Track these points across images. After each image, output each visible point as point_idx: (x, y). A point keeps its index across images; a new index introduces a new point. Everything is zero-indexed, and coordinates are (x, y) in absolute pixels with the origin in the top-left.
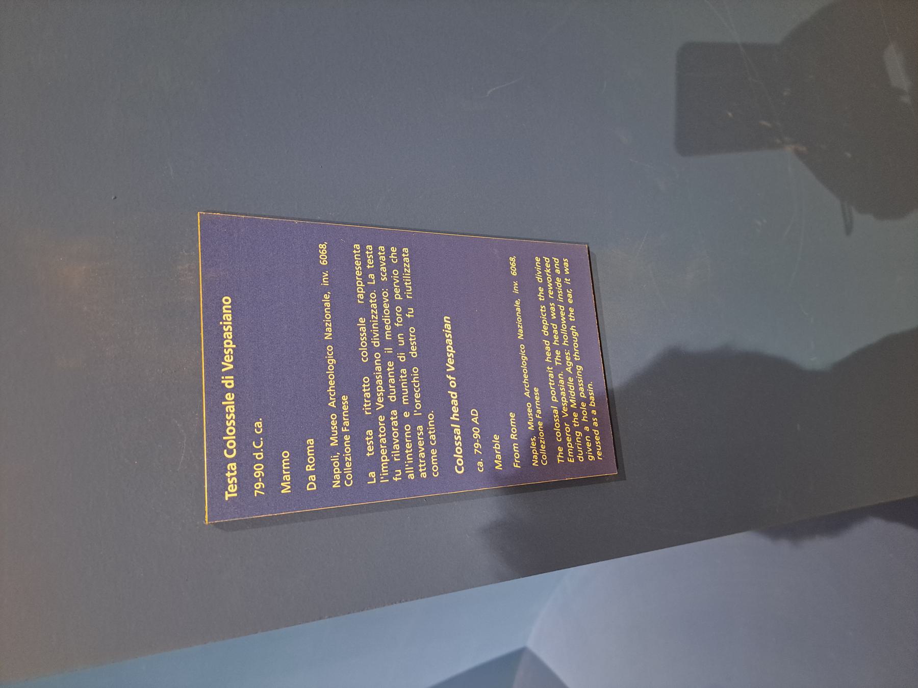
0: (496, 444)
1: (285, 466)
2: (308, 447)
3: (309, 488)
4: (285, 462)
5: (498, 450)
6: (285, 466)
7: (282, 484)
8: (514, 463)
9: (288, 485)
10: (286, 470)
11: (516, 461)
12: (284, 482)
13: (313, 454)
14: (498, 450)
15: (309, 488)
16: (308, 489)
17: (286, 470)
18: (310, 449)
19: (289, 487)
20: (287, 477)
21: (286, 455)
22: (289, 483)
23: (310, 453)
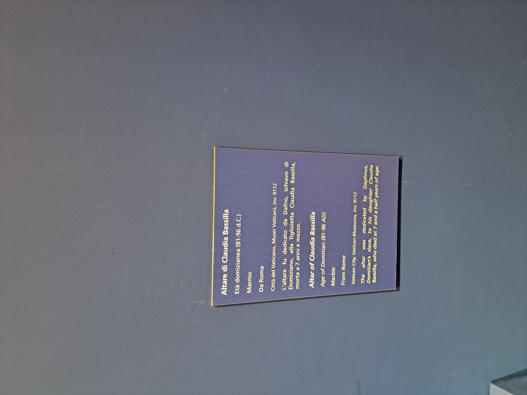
1: (250, 279)
3: (260, 290)
5: (334, 276)
6: (250, 279)
7: (248, 288)
8: (342, 283)
9: (250, 289)
10: (250, 282)
12: (248, 287)
14: (334, 276)
17: (250, 282)
20: (250, 285)
21: (250, 274)
22: (251, 288)
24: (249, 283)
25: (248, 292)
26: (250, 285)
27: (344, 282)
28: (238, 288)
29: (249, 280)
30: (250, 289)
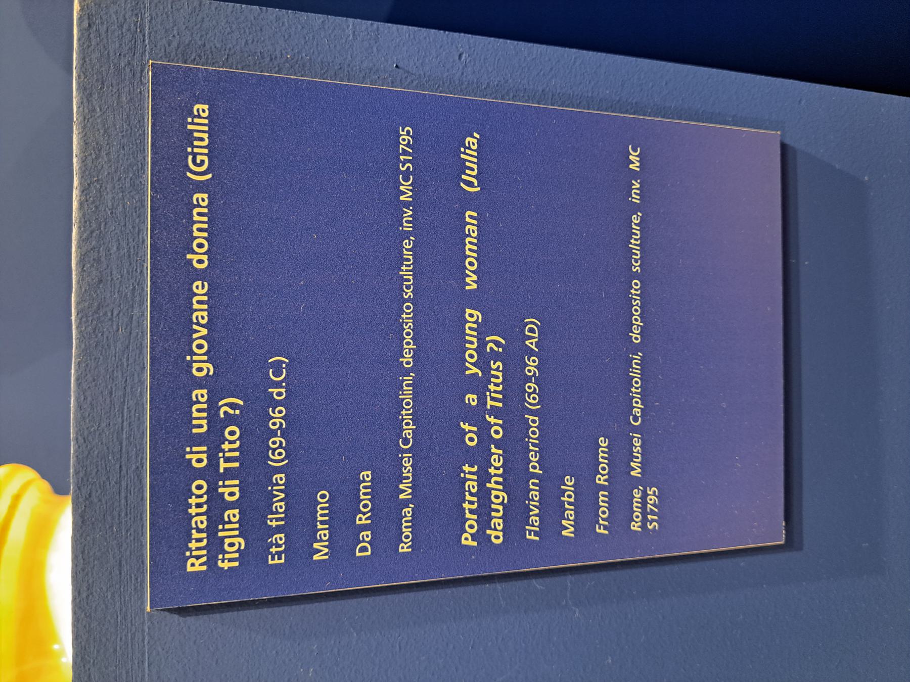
0: (567, 493)
1: (322, 515)
2: (362, 485)
4: (322, 509)
6: (322, 515)
7: (316, 545)
8: (597, 526)
9: (324, 546)
10: (322, 523)
11: (601, 522)
13: (369, 497)
15: (359, 552)
16: (358, 554)
17: (322, 523)
18: (365, 487)
19: (326, 550)
20: (323, 533)
21: (323, 498)
22: (327, 543)
23: (364, 494)
24: (320, 526)
25: (316, 557)
26: (323, 533)
27: (606, 523)
28: (280, 546)
29: (319, 518)
30: (324, 546)
